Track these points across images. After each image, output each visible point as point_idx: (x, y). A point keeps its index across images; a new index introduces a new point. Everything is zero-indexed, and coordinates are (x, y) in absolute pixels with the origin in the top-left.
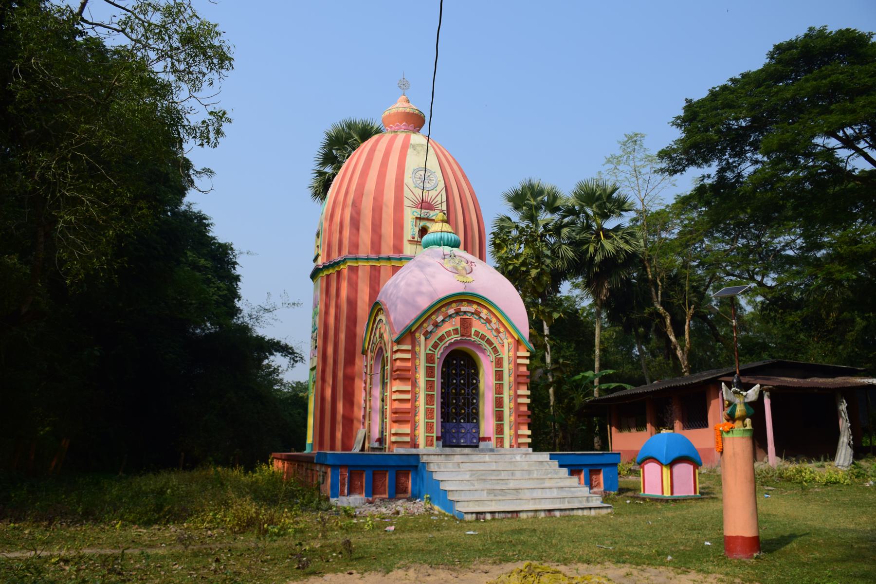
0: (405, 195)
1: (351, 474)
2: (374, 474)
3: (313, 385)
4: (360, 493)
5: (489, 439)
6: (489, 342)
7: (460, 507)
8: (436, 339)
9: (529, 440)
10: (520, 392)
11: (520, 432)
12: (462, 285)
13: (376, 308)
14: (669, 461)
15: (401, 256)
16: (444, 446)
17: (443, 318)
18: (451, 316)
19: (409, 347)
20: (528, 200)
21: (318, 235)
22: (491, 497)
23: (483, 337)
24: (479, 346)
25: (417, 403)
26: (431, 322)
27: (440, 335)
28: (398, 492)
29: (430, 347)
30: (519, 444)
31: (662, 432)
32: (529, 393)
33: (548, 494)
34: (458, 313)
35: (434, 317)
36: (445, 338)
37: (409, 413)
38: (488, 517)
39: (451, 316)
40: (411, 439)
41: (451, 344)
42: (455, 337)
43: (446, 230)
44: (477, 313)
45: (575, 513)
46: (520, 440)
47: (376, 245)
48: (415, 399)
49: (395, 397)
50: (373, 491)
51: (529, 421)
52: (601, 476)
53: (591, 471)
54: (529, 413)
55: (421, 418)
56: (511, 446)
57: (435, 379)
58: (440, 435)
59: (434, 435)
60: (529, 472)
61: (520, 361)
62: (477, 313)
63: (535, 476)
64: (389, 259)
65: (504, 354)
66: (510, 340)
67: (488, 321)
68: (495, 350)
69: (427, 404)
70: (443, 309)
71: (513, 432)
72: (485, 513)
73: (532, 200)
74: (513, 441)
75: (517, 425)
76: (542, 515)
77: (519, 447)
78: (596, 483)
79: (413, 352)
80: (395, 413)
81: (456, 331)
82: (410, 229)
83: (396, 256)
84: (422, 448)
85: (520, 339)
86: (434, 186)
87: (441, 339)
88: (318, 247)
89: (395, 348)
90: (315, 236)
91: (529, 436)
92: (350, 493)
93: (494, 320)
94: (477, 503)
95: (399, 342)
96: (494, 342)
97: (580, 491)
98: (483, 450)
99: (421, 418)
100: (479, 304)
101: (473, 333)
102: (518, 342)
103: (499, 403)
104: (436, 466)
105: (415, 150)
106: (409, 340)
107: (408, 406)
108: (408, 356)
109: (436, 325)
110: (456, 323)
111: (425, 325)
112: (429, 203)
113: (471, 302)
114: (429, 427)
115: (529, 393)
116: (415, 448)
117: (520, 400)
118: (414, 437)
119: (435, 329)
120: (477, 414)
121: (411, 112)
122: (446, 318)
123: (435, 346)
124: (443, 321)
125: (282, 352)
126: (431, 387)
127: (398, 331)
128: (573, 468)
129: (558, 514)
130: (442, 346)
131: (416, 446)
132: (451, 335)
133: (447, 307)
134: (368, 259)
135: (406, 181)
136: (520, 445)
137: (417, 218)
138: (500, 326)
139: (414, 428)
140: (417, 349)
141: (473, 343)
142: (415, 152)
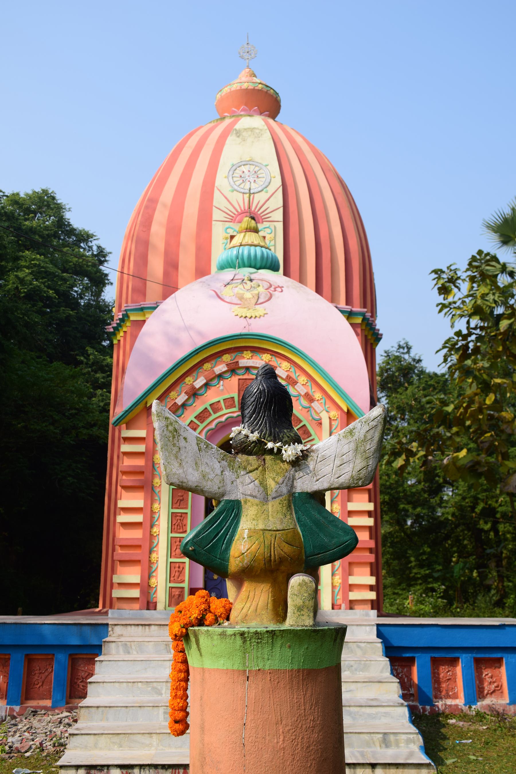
0: (215, 203)
8: (192, 418)
9: (372, 595)
11: (353, 580)
17: (205, 381)
19: (142, 433)
25: (155, 529)
27: (200, 409)
30: (351, 602)
32: (370, 507)
34: (233, 369)
35: (189, 380)
36: (210, 415)
37: (139, 546)
39: (220, 376)
40: (142, 592)
43: (250, 242)
46: (354, 595)
51: (371, 558)
53: (477, 661)
59: (185, 585)
66: (334, 413)
72: (108, 766)
74: (339, 597)
77: (351, 608)
78: (493, 687)
81: (229, 402)
85: (353, 410)
86: (264, 186)
87: (202, 416)
91: (371, 588)
93: (302, 379)
94: (116, 739)
96: (301, 417)
97: (386, 714)
104: (121, 649)
105: (238, 137)
109: (194, 393)
111: (173, 394)
113: (256, 350)
115: (370, 507)
116: (148, 609)
119: (191, 401)
121: (250, 88)
122: (211, 380)
124: (207, 385)
126: (181, 500)
128: (436, 655)
132: (221, 409)
133: (213, 362)
135: (217, 184)
138: (315, 389)
142: (239, 140)
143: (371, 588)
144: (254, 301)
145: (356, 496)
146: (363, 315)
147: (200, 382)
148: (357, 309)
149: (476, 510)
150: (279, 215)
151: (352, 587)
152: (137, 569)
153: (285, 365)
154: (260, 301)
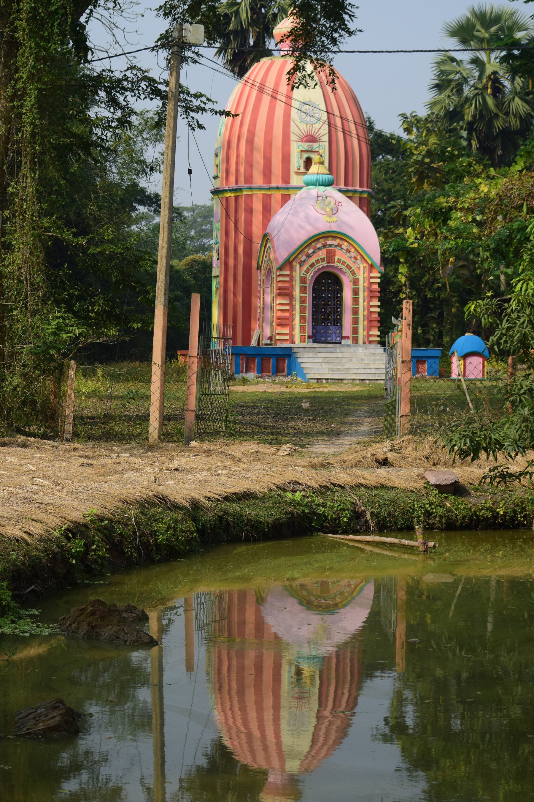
0: (292, 130)
1: (247, 359)
2: (262, 360)
3: (216, 291)
4: (254, 372)
5: (348, 338)
6: (349, 267)
7: (308, 376)
9: (378, 339)
10: (372, 304)
11: (371, 333)
12: (328, 224)
13: (266, 238)
14: (463, 354)
15: (288, 186)
16: (314, 342)
19: (288, 273)
20: (478, 31)
21: (217, 155)
22: (331, 372)
23: (344, 263)
24: (341, 270)
26: (304, 253)
28: (278, 371)
29: (303, 272)
31: (467, 334)
32: (379, 304)
33: (368, 371)
34: (324, 246)
35: (306, 250)
38: (324, 381)
39: (319, 249)
41: (319, 269)
42: (321, 265)
44: (339, 245)
45: (379, 382)
46: (371, 339)
47: (267, 173)
48: (292, 308)
49: (278, 308)
50: (262, 370)
51: (378, 324)
52: (426, 366)
53: (417, 361)
54: (379, 319)
55: (297, 322)
56: (364, 343)
57: (307, 295)
58: (311, 334)
59: (306, 334)
61: (372, 280)
62: (339, 245)
63: (366, 362)
64: (278, 188)
66: (365, 265)
67: (348, 251)
68: (353, 273)
69: (301, 313)
70: (314, 244)
71: (365, 333)
73: (483, 31)
74: (366, 339)
75: (369, 328)
76: (358, 382)
79: (291, 276)
80: (279, 319)
81: (323, 260)
83: (284, 186)
84: (297, 343)
87: (312, 265)
88: (217, 166)
89: (278, 274)
90: (213, 155)
91: (378, 336)
92: (247, 371)
93: (353, 250)
95: (281, 269)
98: (343, 345)
99: (297, 322)
100: (341, 239)
101: (336, 260)
102: (372, 267)
103: (355, 312)
106: (288, 267)
107: (287, 314)
108: (287, 279)
109: (308, 256)
110: (322, 254)
111: (300, 256)
112: (313, 136)
114: (302, 329)
115: (379, 304)
117: (372, 310)
118: (291, 335)
120: (341, 319)
123: (307, 271)
124: (313, 252)
125: (149, 206)
127: (281, 261)
129: (367, 382)
130: (312, 271)
131: (293, 342)
134: (260, 189)
136: (370, 342)
137: (302, 151)
139: (292, 329)
140: (294, 273)
141: (336, 268)
143: (378, 336)
144: (331, 213)
145: (374, 300)
146: (368, 192)
147: (311, 251)
148: (365, 189)
149: (423, 280)
150: (326, 138)
153: (346, 244)
154: (334, 212)
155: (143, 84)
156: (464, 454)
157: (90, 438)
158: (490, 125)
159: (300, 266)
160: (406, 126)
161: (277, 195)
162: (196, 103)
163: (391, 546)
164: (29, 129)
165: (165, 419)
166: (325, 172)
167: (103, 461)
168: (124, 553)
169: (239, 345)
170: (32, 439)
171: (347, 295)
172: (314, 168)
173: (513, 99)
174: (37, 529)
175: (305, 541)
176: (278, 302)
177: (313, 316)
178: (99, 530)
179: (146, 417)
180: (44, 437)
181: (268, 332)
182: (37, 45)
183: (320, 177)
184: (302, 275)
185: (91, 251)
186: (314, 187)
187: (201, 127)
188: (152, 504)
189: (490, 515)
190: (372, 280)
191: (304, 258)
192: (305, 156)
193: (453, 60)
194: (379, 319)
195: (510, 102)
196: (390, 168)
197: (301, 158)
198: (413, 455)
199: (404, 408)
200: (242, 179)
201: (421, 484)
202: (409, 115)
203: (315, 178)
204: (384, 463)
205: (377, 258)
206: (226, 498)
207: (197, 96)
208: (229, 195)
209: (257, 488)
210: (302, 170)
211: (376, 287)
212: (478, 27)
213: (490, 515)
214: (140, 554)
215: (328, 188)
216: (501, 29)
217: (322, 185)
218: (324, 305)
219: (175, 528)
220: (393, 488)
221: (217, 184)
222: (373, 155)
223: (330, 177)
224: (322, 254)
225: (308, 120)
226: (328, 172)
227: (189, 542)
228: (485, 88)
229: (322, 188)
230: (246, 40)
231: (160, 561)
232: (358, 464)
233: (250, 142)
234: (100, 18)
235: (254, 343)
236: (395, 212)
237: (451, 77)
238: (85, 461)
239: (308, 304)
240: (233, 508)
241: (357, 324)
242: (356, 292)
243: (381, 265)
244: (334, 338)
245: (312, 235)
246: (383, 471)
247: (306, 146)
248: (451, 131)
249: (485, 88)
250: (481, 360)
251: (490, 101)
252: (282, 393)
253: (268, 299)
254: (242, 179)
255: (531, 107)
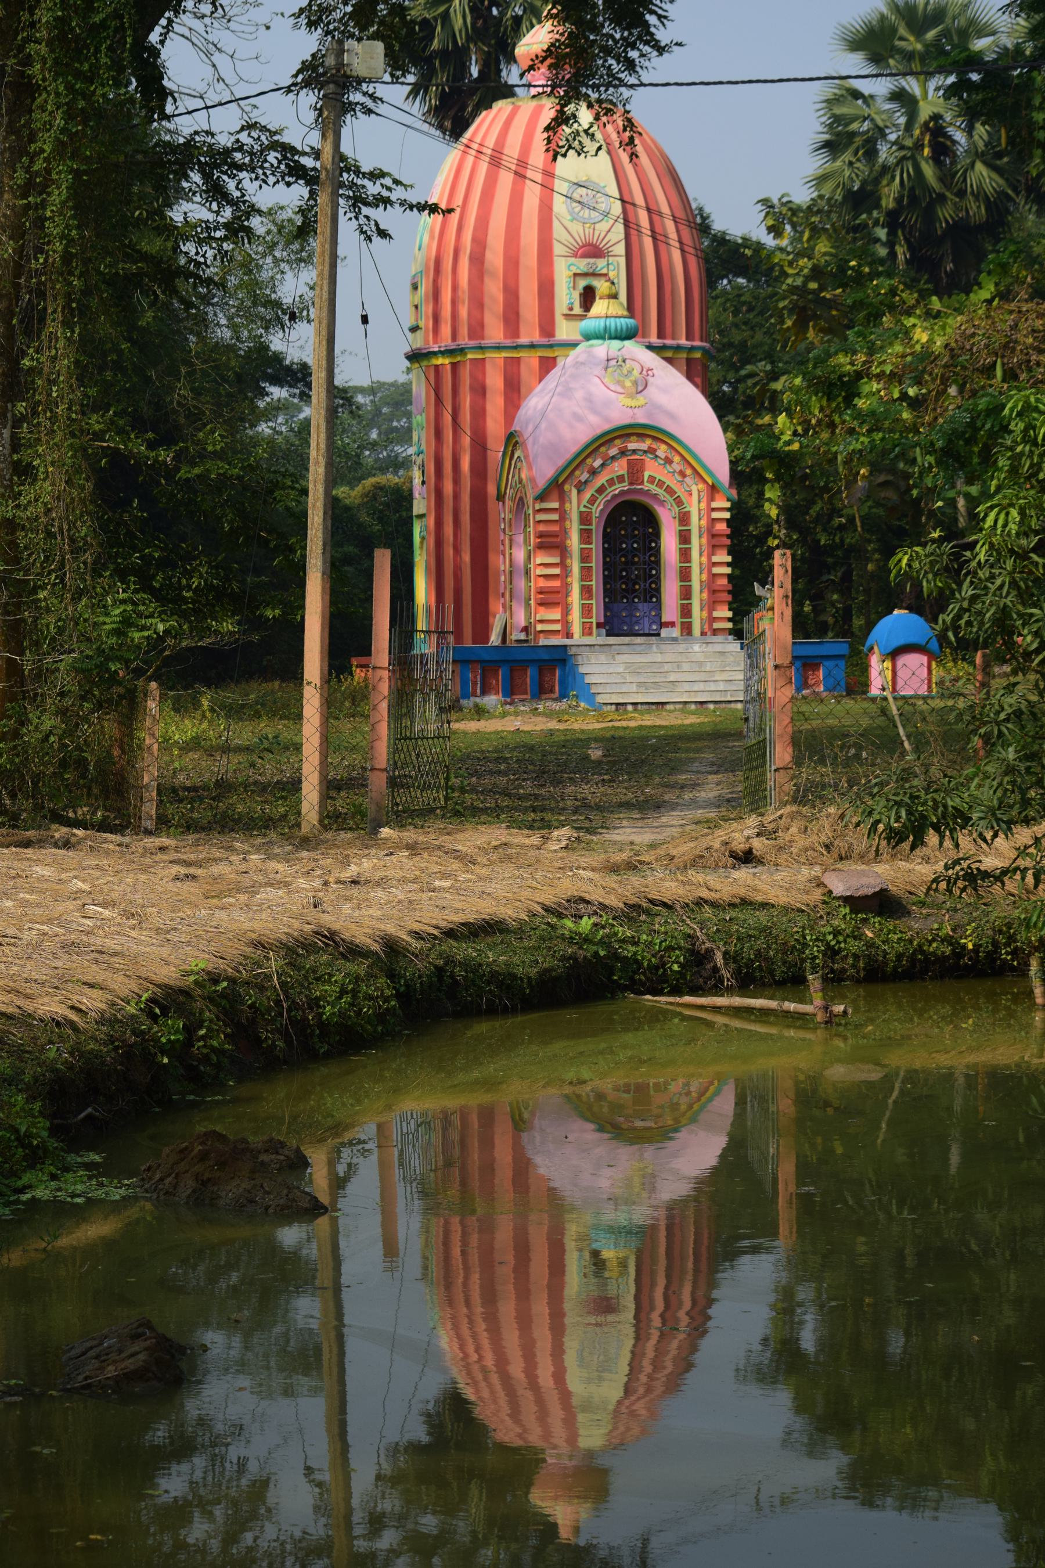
0: (555, 235)
1: (483, 670)
2: (512, 670)
3: (422, 543)
4: (497, 693)
5: (672, 624)
6: (670, 491)
7: (600, 699)
9: (730, 625)
10: (715, 559)
11: (716, 614)
13: (512, 441)
14: (890, 649)
15: (552, 341)
16: (608, 635)
18: (613, 458)
20: (902, 39)
21: (415, 287)
22: (643, 690)
23: (660, 484)
24: (655, 497)
26: (585, 468)
27: (599, 485)
28: (542, 691)
29: (585, 502)
31: (896, 612)
32: (729, 559)
33: (713, 687)
34: (623, 452)
35: (589, 461)
38: (630, 708)
39: (613, 458)
41: (615, 497)
44: (652, 451)
45: (733, 705)
46: (716, 626)
47: (512, 319)
49: (539, 572)
50: (511, 691)
51: (729, 597)
52: (821, 673)
53: (804, 665)
54: (730, 587)
56: (703, 634)
57: (593, 546)
59: (594, 620)
60: (701, 663)
62: (652, 451)
64: (532, 346)
65: (691, 506)
66: (701, 486)
67: (669, 461)
68: (679, 502)
69: (582, 580)
70: (603, 449)
71: (705, 614)
73: (912, 39)
74: (706, 626)
75: (712, 605)
76: (693, 707)
80: (541, 593)
81: (621, 479)
82: (566, 296)
83: (544, 341)
87: (601, 490)
88: (416, 307)
89: (537, 507)
90: (408, 286)
91: (729, 620)
92: (484, 692)
95: (542, 497)
98: (663, 639)
101: (646, 478)
102: (713, 489)
103: (685, 575)
106: (555, 494)
107: (556, 583)
108: (555, 517)
109: (593, 472)
110: (620, 468)
111: (577, 473)
113: (642, 436)
114: (586, 611)
115: (729, 559)
117: (716, 570)
118: (565, 622)
120: (658, 590)
123: (592, 501)
124: (603, 465)
125: (291, 386)
127: (542, 483)
129: (711, 706)
130: (601, 500)
131: (569, 635)
134: (498, 348)
136: (715, 632)
137: (575, 275)
139: (566, 612)
140: (567, 506)
141: (647, 493)
143: (729, 620)
144: (634, 390)
146: (703, 349)
147: (597, 463)
148: (697, 343)
149: (811, 512)
150: (620, 249)
151: (716, 619)
152: (559, 610)
153: (663, 447)
154: (640, 388)
155: (272, 157)
156: (895, 837)
157: (190, 826)
158: (929, 215)
159: (579, 492)
160: (771, 222)
161: (530, 360)
162: (373, 189)
163: (764, 1014)
164: (58, 246)
165: (331, 787)
166: (620, 313)
167: (215, 870)
168: (259, 1041)
169: (468, 644)
170: (80, 833)
171: (669, 543)
172: (600, 307)
173: (972, 165)
174: (94, 1001)
175: (602, 1009)
176: (539, 561)
177: (605, 584)
178: (211, 1000)
179: (295, 785)
180: (104, 827)
181: (520, 618)
182: (69, 87)
183: (612, 323)
184: (583, 509)
185: (182, 474)
186: (600, 342)
187: (383, 234)
188: (310, 948)
189: (948, 950)
190: (715, 515)
191: (585, 476)
192: (582, 283)
193: (856, 94)
194: (730, 587)
195: (965, 171)
196: (744, 303)
197: (574, 288)
198: (801, 842)
199: (782, 754)
200: (464, 331)
201: (817, 895)
202: (775, 201)
203: (602, 324)
204: (747, 858)
205: (722, 472)
206: (450, 933)
207: (376, 175)
208: (440, 361)
209: (508, 913)
210: (578, 310)
211: (722, 527)
212: (902, 31)
213: (948, 950)
214: (289, 1042)
215: (627, 343)
216: (946, 34)
217: (616, 338)
218: (626, 563)
219: (355, 993)
220: (764, 905)
221: (418, 341)
222: (710, 280)
223: (631, 322)
224: (620, 468)
225: (586, 215)
226: (625, 313)
227: (381, 1017)
228: (919, 146)
229: (616, 344)
230: (464, 68)
231: (328, 1055)
232: (697, 862)
233: (478, 259)
234: (187, 33)
235: (495, 639)
236: (755, 384)
237: (854, 126)
238: (183, 870)
239: (596, 563)
240: (464, 951)
241: (690, 598)
242: (685, 538)
243: (731, 486)
244: (645, 626)
245: (599, 432)
246: (743, 874)
247: (582, 265)
248: (855, 229)
249: (919, 146)
250: (924, 659)
251: (929, 171)
252: (551, 732)
253: (520, 555)
254: (464, 331)
255: (1007, 180)
